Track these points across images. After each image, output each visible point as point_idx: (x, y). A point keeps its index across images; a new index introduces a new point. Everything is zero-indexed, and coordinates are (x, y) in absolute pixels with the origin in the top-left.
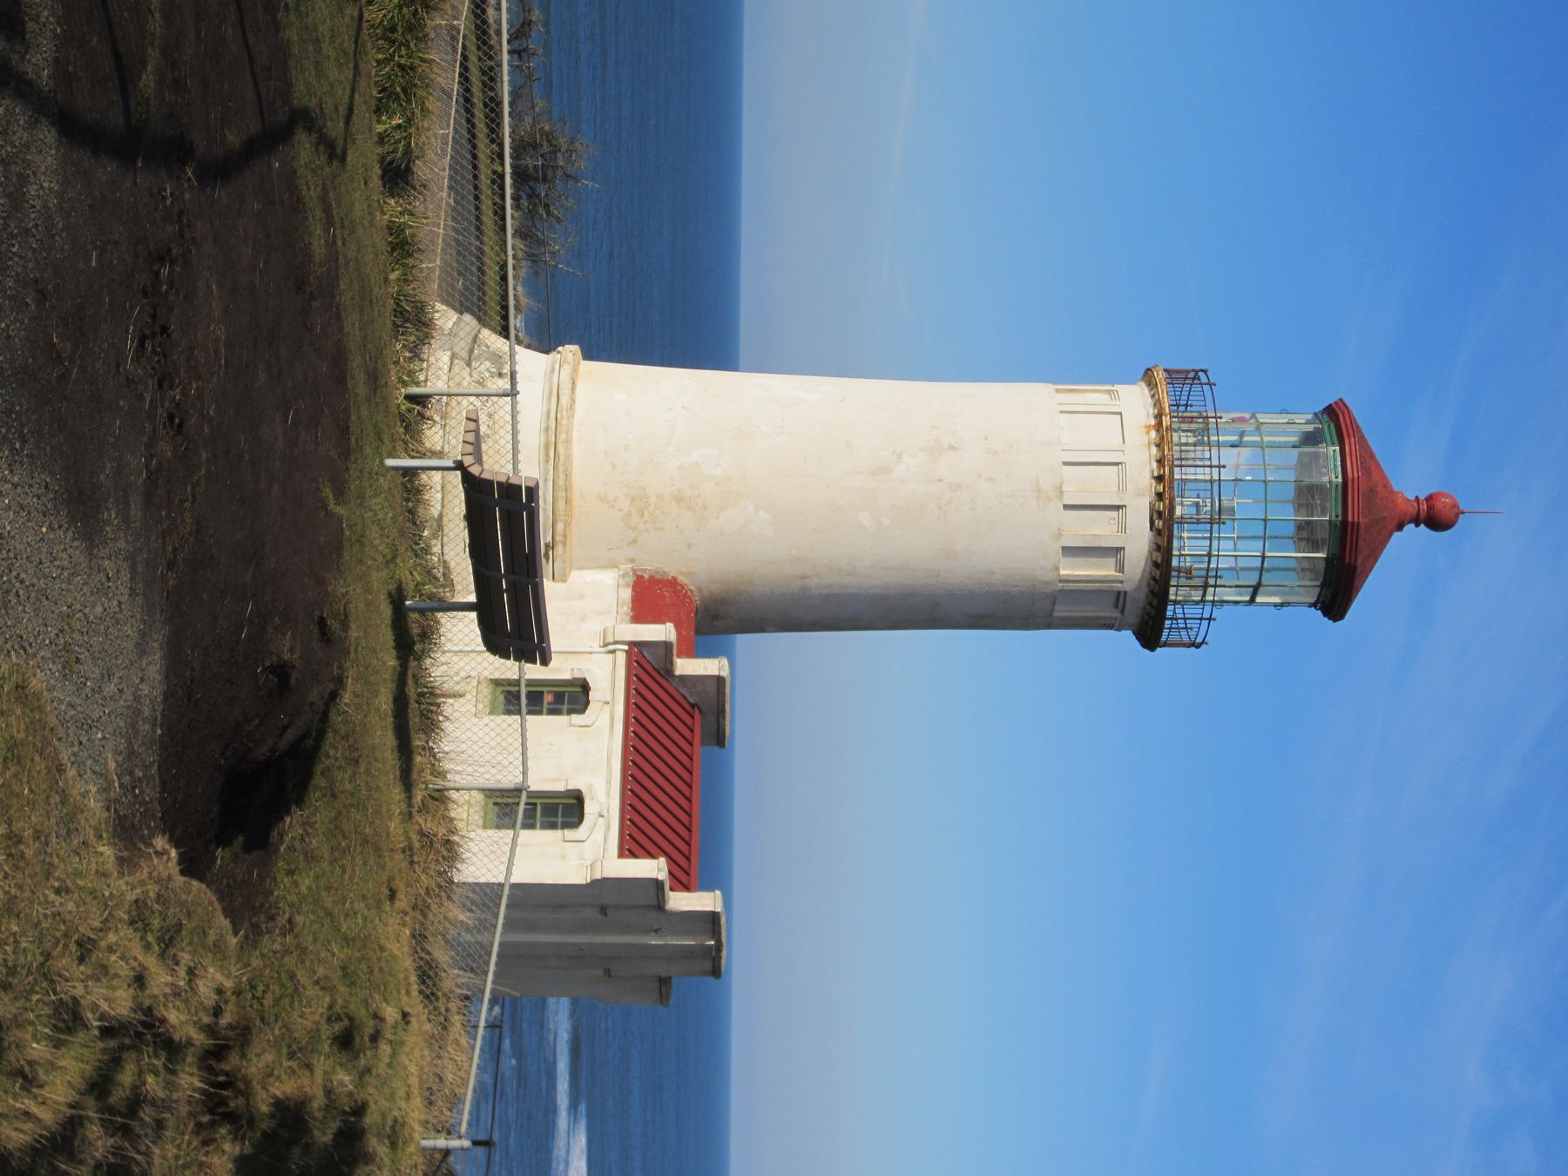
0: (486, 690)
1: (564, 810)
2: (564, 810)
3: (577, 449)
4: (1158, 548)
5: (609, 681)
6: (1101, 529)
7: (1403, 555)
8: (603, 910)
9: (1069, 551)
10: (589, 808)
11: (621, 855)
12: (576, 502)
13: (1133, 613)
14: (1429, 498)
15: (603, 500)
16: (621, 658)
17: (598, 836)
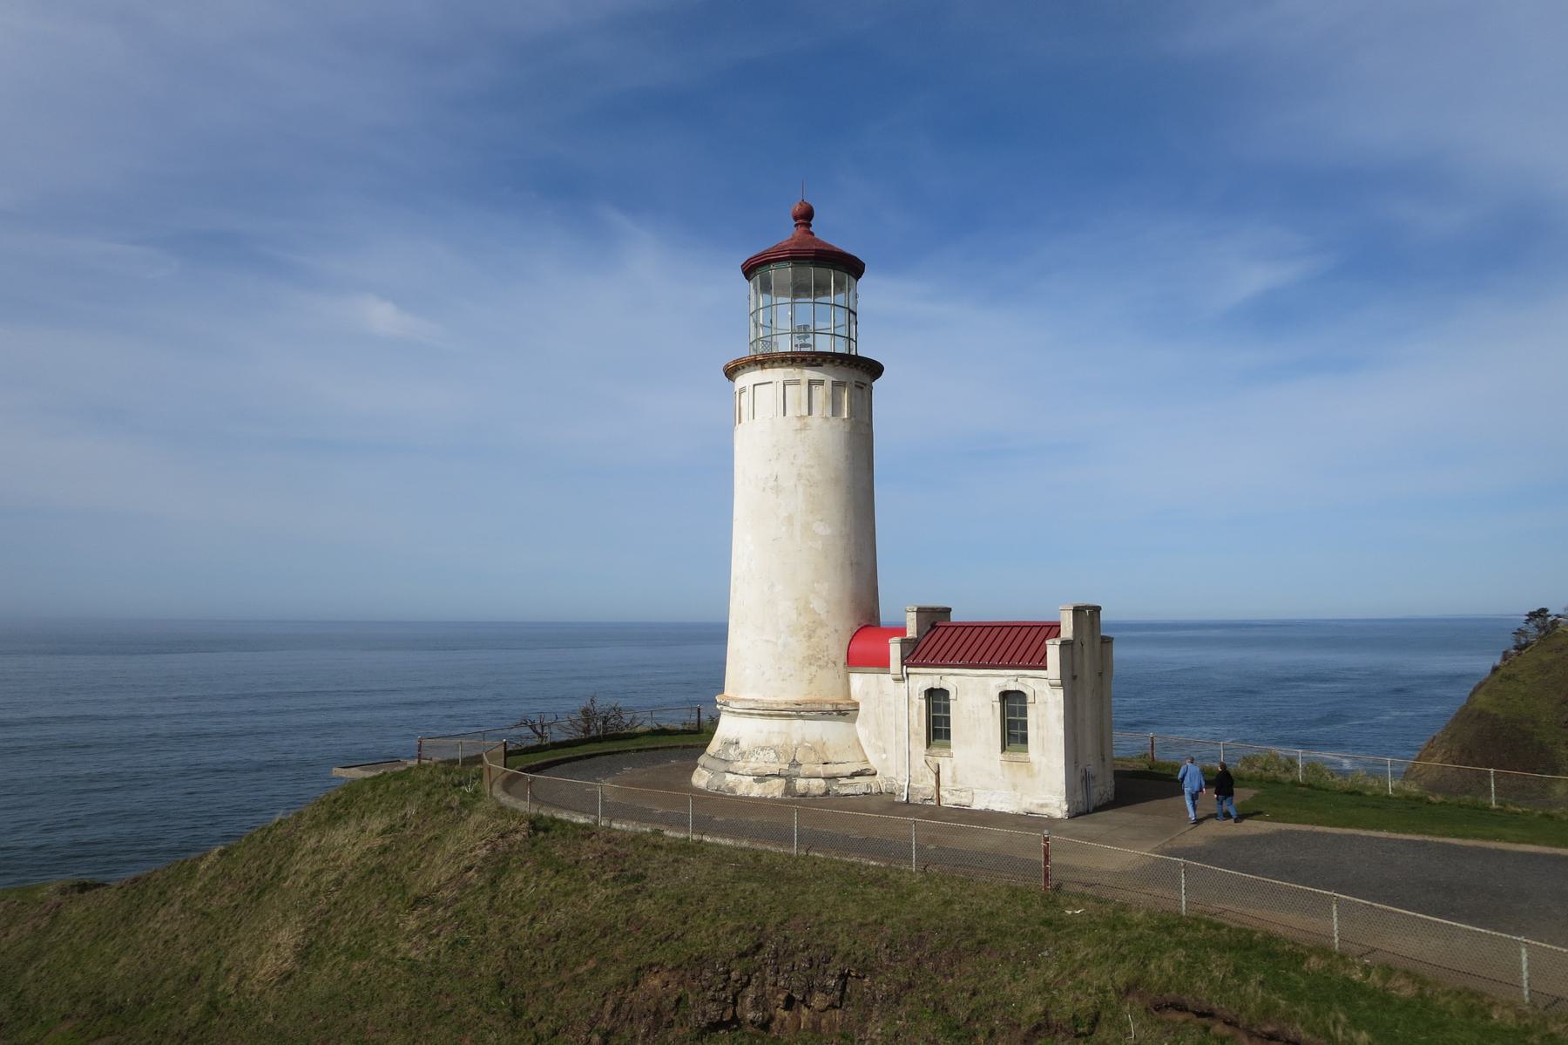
0: (934, 751)
1: (1013, 703)
2: (1013, 703)
3: (781, 698)
4: (832, 362)
5: (925, 679)
6: (820, 394)
7: (830, 231)
8: (1074, 678)
9: (836, 411)
10: (1012, 687)
11: (1045, 668)
12: (813, 697)
13: (866, 379)
14: (796, 218)
15: (811, 681)
16: (910, 670)
17: (1030, 682)
